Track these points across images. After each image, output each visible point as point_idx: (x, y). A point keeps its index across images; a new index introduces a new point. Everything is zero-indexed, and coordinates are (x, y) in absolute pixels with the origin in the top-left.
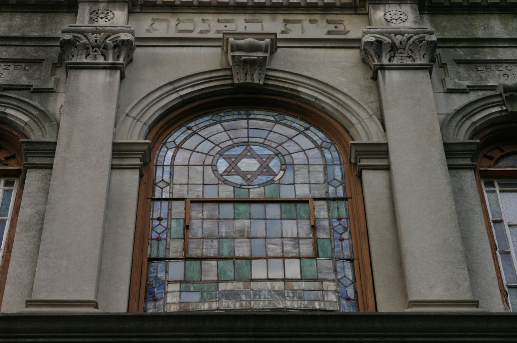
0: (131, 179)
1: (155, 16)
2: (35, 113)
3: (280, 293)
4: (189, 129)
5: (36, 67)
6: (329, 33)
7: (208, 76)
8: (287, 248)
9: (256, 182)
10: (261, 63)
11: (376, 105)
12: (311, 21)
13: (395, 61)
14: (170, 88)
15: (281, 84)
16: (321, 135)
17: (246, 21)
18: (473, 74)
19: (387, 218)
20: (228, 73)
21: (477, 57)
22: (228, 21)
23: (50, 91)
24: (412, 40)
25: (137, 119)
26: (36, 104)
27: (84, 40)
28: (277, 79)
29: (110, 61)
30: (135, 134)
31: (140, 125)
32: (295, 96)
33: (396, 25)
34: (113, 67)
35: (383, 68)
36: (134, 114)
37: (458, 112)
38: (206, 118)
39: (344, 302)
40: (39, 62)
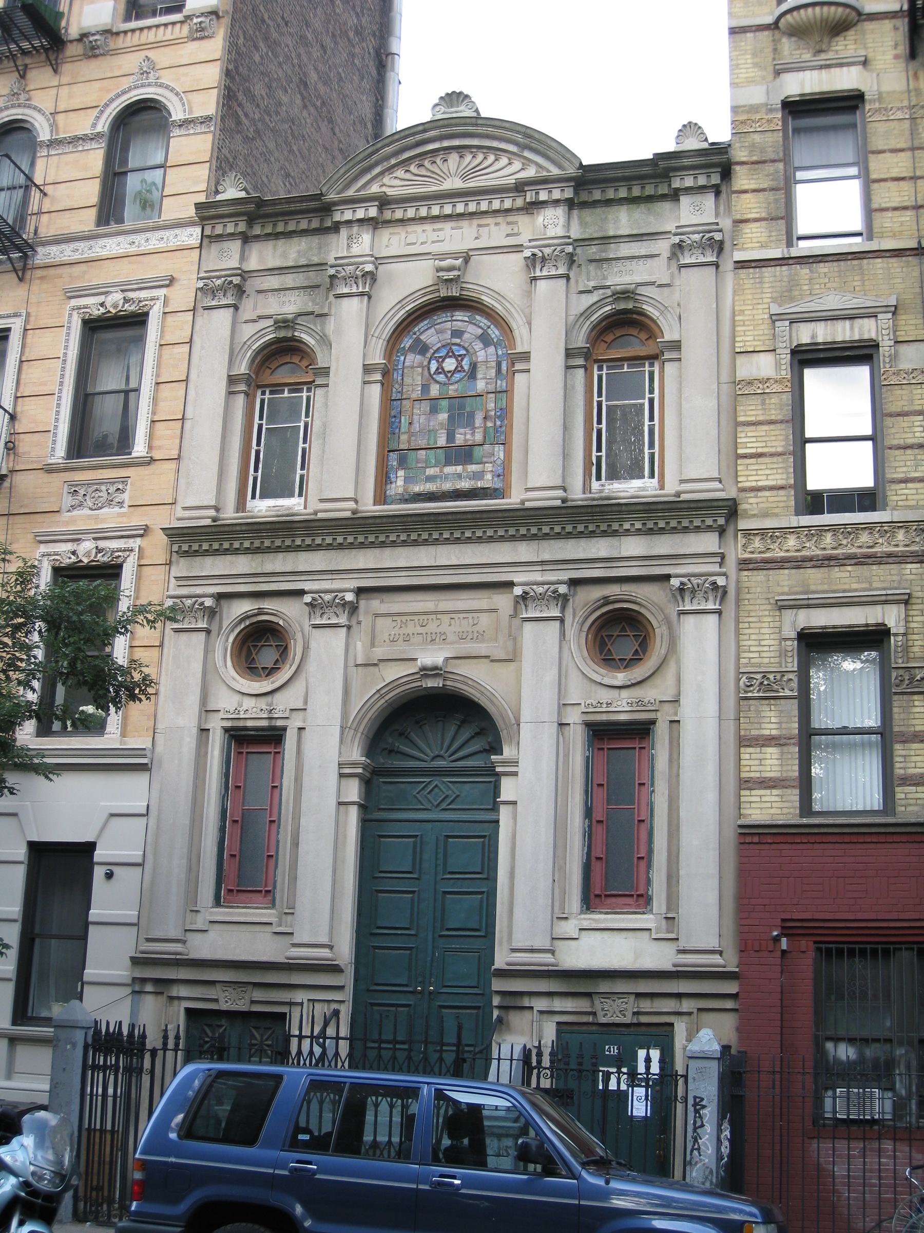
0: (376, 389)
1: (391, 230)
2: (318, 338)
3: (459, 476)
4: (415, 334)
5: (317, 290)
6: (508, 235)
7: (423, 291)
8: (468, 437)
9: (453, 379)
10: (456, 280)
12: (497, 224)
13: (545, 273)
14: (399, 305)
15: (471, 294)
16: (497, 332)
17: (452, 229)
18: (599, 273)
20: (436, 287)
21: (604, 255)
22: (440, 230)
23: (325, 315)
24: (556, 253)
25: (379, 338)
27: (343, 274)
28: (468, 290)
29: (360, 290)
31: (381, 341)
33: (551, 232)
34: (362, 294)
36: (376, 335)
37: (582, 314)
38: (426, 322)
39: (496, 479)
40: (318, 286)
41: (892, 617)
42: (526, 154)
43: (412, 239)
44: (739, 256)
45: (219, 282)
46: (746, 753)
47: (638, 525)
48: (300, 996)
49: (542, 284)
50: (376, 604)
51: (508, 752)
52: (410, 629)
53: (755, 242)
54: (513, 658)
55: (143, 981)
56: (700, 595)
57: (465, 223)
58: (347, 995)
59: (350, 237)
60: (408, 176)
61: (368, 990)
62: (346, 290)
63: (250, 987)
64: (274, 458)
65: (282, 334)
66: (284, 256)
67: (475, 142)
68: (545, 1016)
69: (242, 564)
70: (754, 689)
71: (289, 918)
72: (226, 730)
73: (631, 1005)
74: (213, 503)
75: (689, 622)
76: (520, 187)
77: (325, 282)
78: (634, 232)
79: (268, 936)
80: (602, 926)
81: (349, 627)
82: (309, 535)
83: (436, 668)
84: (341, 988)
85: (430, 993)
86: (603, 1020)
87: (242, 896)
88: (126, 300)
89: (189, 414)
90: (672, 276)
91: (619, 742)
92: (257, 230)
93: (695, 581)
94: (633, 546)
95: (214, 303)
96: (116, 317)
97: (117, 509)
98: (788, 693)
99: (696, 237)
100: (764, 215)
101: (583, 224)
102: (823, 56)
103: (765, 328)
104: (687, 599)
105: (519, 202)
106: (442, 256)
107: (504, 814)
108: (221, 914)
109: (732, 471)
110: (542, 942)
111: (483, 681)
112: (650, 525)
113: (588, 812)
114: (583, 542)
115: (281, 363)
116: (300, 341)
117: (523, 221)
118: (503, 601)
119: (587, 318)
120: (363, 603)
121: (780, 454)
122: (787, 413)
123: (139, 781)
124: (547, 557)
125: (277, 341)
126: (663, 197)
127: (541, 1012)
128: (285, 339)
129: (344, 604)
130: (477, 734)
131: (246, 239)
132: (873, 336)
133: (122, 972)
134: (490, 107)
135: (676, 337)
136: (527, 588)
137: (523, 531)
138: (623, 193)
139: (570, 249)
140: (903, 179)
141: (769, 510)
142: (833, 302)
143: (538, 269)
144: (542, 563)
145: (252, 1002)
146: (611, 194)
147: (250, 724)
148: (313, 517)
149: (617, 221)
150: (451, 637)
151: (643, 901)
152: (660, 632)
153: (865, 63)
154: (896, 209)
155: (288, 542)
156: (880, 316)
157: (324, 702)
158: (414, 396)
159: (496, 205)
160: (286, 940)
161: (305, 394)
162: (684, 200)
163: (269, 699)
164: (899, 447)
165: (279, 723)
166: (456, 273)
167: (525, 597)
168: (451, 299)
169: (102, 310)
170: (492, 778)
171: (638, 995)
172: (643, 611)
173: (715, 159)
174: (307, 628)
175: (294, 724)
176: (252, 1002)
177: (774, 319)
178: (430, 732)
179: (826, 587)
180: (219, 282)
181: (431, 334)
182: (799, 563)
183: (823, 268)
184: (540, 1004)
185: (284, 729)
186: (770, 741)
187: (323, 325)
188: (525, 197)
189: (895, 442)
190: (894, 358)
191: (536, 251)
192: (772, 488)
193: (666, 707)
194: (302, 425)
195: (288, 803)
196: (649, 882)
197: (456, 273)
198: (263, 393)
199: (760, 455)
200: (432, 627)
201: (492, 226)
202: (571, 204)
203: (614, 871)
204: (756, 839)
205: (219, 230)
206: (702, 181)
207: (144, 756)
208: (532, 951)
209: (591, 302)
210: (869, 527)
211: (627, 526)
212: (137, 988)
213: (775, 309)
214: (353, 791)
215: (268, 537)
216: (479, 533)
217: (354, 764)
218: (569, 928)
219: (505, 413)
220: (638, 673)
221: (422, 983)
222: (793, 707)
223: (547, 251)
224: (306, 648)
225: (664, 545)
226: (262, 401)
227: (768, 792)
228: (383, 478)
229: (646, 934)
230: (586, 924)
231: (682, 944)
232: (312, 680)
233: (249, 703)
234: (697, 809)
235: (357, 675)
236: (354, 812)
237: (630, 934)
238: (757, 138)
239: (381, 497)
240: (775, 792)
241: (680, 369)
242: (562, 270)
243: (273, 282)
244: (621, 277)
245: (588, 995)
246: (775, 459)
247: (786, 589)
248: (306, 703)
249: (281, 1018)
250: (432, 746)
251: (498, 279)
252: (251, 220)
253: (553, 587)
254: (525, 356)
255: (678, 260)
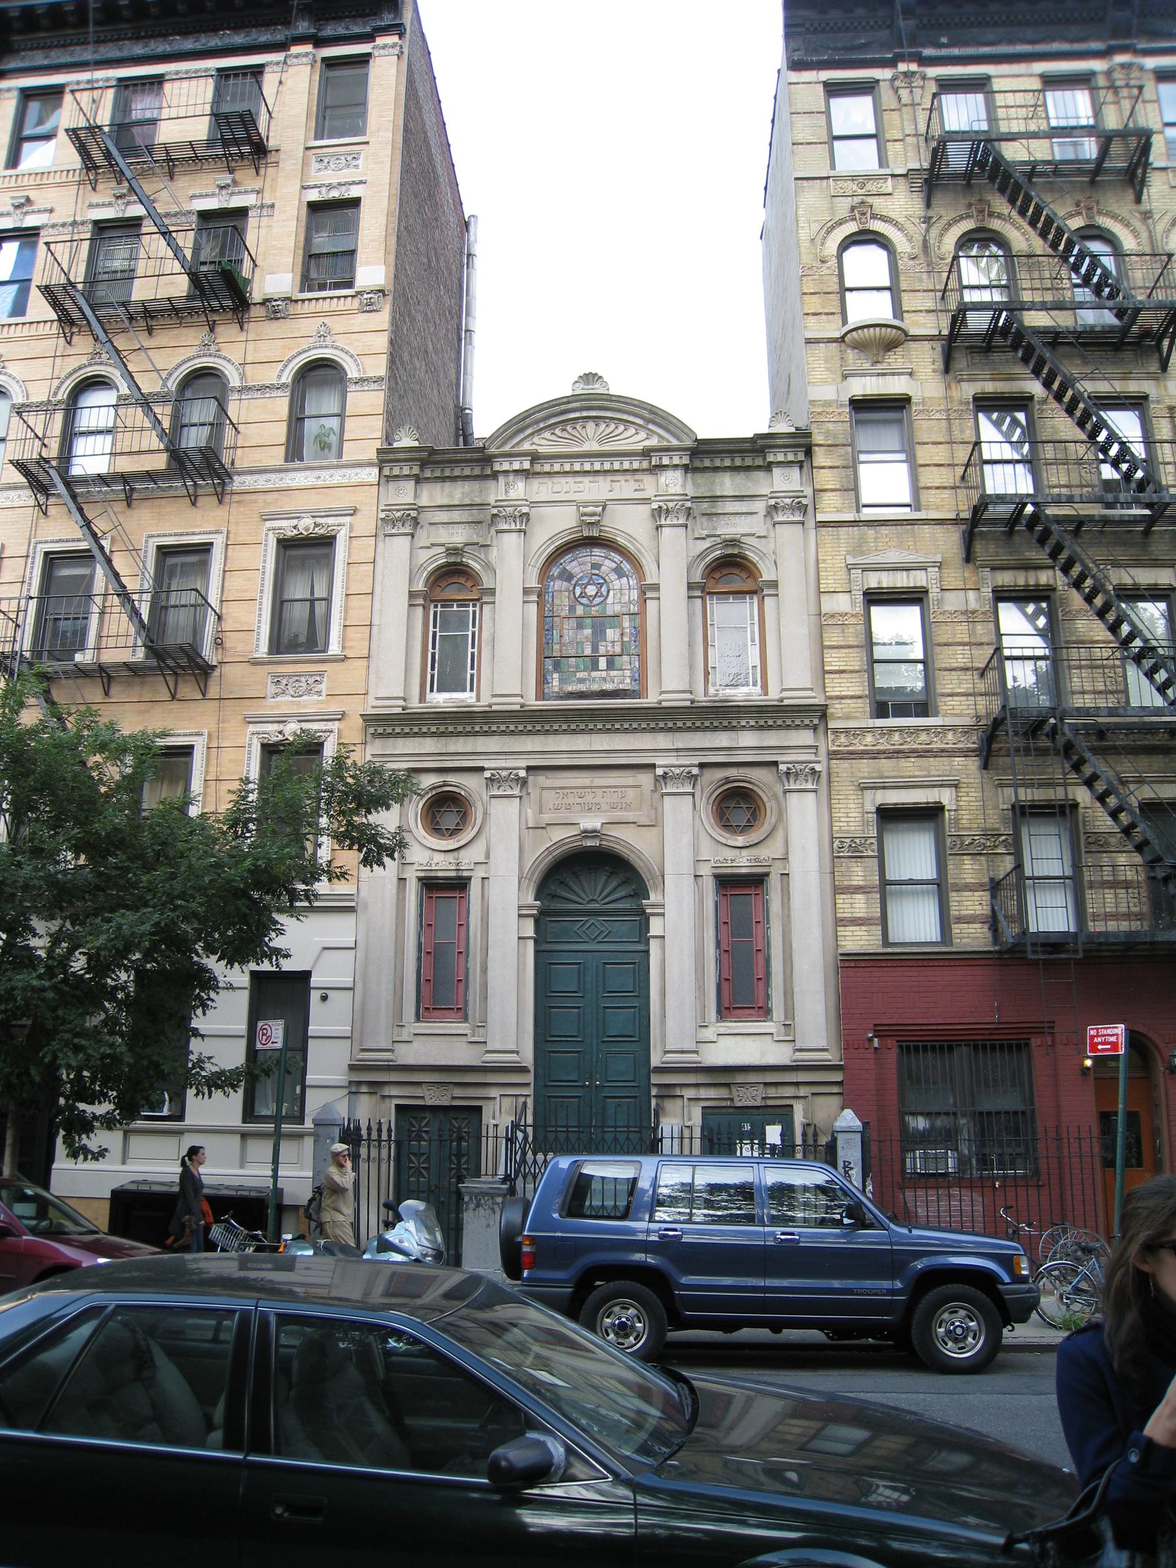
0: (533, 608)
1: (540, 480)
3: (604, 679)
11: (655, 551)
13: (668, 522)
19: (657, 634)
21: (714, 511)
26: (483, 557)
28: (606, 532)
30: (533, 583)
32: (614, 542)
33: (672, 490)
34: (520, 531)
35: (661, 526)
40: (481, 522)
41: (945, 797)
42: (651, 426)
43: (557, 488)
44: (820, 517)
45: (399, 514)
46: (840, 899)
47: (752, 723)
48: (494, 1092)
49: (666, 531)
50: (542, 779)
51: (654, 897)
52: (570, 800)
53: (832, 508)
54: (655, 823)
55: (359, 1083)
56: (802, 778)
57: (600, 478)
58: (529, 1091)
59: (507, 484)
60: (553, 438)
61: (546, 1086)
62: (506, 527)
63: (451, 1086)
64: (450, 662)
65: (452, 559)
66: (451, 495)
67: (609, 414)
68: (692, 1103)
69: (429, 745)
70: (841, 851)
71: (481, 1029)
72: (420, 879)
73: (760, 1092)
74: (402, 695)
75: (793, 799)
76: (646, 453)
77: (489, 519)
78: (737, 494)
79: (465, 1045)
80: (735, 1031)
81: (521, 797)
82: (486, 723)
83: (595, 831)
84: (528, 1084)
85: (597, 1086)
86: (739, 1104)
87: (438, 1013)
88: (316, 525)
89: (376, 621)
90: (768, 530)
91: (740, 890)
92: (428, 474)
93: (798, 767)
94: (748, 739)
95: (394, 531)
96: (307, 538)
97: (316, 697)
98: (871, 854)
99: (788, 501)
100: (838, 487)
101: (695, 485)
102: (879, 366)
103: (842, 574)
104: (792, 781)
105: (645, 465)
106: (586, 504)
107: (654, 946)
108: (423, 1027)
109: (821, 683)
110: (689, 1045)
111: (633, 842)
112: (762, 723)
113: (718, 945)
114: (709, 735)
115: (452, 584)
116: (467, 566)
117: (648, 481)
118: (645, 779)
119: (703, 559)
120: (531, 779)
121: (857, 672)
122: (861, 640)
123: (348, 920)
124: (680, 746)
125: (448, 564)
126: (759, 468)
127: (689, 1099)
128: (454, 564)
129: (518, 779)
130: (624, 883)
131: (418, 480)
132: (924, 584)
133: (340, 1076)
134: (617, 387)
135: (774, 578)
136: (666, 770)
137: (661, 725)
138: (728, 463)
139: (688, 504)
140: (942, 465)
141: (851, 712)
142: (894, 556)
143: (663, 518)
144: (677, 750)
145: (453, 1098)
146: (718, 463)
147: (440, 874)
148: (487, 709)
149: (722, 484)
150: (604, 807)
151: (765, 1012)
152: (770, 805)
153: (911, 374)
154: (938, 488)
155: (468, 729)
156: (929, 569)
157: (503, 856)
158: (563, 614)
159: (626, 466)
160: (482, 1048)
161: (471, 609)
162: (776, 471)
163: (455, 854)
164: (946, 670)
165: (465, 874)
166: (597, 518)
167: (665, 776)
168: (590, 539)
169: (295, 532)
170: (643, 919)
171: (766, 1084)
172: (755, 788)
173: (802, 441)
174: (485, 798)
175: (479, 873)
176: (453, 1098)
177: (849, 568)
178: (589, 882)
179: (895, 774)
180: (399, 514)
181: (576, 564)
182: (875, 755)
183: (884, 530)
184: (689, 1093)
185: (469, 878)
186: (858, 889)
187: (486, 554)
188: (650, 461)
189: (943, 666)
190: (940, 602)
191: (662, 504)
192: (852, 697)
193: (778, 864)
194: (470, 633)
195: (475, 937)
196: (768, 997)
197: (597, 518)
198: (436, 606)
199: (842, 672)
200: (589, 798)
201: (623, 482)
202: (686, 468)
203: (742, 989)
204: (852, 964)
205: (396, 471)
206: (791, 457)
207: (352, 900)
208: (683, 1052)
209: (705, 547)
210: (927, 729)
211: (743, 723)
212: (354, 1090)
213: (850, 560)
214: (529, 929)
215: (451, 724)
216: (626, 726)
217: (530, 907)
218: (709, 1034)
219: (640, 633)
220: (754, 837)
221: (590, 1079)
222: (874, 863)
223: (671, 505)
224: (485, 813)
225: (772, 738)
226: (435, 613)
227: (858, 928)
228: (542, 679)
229: (769, 1037)
230: (722, 1031)
231: (798, 1045)
232: (492, 839)
233: (439, 858)
234: (806, 939)
235: (529, 837)
236: (531, 944)
237: (757, 1037)
238: (831, 426)
239: (541, 695)
240: (863, 928)
241: (778, 602)
242: (682, 521)
243: (443, 516)
244: (729, 528)
245: (728, 1085)
246: (853, 675)
247: (866, 775)
248: (488, 856)
249: (478, 1110)
250: (595, 891)
251: (630, 524)
252: (423, 464)
253: (687, 769)
254: (656, 587)
255: (772, 518)
